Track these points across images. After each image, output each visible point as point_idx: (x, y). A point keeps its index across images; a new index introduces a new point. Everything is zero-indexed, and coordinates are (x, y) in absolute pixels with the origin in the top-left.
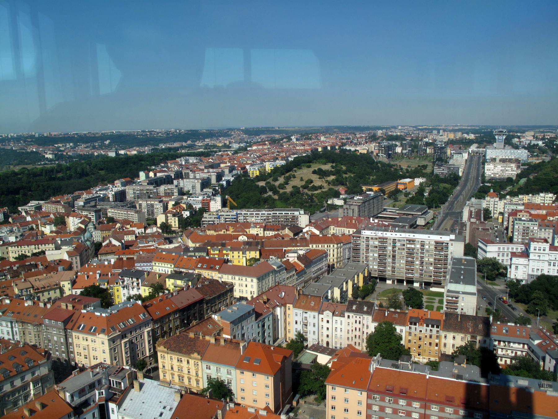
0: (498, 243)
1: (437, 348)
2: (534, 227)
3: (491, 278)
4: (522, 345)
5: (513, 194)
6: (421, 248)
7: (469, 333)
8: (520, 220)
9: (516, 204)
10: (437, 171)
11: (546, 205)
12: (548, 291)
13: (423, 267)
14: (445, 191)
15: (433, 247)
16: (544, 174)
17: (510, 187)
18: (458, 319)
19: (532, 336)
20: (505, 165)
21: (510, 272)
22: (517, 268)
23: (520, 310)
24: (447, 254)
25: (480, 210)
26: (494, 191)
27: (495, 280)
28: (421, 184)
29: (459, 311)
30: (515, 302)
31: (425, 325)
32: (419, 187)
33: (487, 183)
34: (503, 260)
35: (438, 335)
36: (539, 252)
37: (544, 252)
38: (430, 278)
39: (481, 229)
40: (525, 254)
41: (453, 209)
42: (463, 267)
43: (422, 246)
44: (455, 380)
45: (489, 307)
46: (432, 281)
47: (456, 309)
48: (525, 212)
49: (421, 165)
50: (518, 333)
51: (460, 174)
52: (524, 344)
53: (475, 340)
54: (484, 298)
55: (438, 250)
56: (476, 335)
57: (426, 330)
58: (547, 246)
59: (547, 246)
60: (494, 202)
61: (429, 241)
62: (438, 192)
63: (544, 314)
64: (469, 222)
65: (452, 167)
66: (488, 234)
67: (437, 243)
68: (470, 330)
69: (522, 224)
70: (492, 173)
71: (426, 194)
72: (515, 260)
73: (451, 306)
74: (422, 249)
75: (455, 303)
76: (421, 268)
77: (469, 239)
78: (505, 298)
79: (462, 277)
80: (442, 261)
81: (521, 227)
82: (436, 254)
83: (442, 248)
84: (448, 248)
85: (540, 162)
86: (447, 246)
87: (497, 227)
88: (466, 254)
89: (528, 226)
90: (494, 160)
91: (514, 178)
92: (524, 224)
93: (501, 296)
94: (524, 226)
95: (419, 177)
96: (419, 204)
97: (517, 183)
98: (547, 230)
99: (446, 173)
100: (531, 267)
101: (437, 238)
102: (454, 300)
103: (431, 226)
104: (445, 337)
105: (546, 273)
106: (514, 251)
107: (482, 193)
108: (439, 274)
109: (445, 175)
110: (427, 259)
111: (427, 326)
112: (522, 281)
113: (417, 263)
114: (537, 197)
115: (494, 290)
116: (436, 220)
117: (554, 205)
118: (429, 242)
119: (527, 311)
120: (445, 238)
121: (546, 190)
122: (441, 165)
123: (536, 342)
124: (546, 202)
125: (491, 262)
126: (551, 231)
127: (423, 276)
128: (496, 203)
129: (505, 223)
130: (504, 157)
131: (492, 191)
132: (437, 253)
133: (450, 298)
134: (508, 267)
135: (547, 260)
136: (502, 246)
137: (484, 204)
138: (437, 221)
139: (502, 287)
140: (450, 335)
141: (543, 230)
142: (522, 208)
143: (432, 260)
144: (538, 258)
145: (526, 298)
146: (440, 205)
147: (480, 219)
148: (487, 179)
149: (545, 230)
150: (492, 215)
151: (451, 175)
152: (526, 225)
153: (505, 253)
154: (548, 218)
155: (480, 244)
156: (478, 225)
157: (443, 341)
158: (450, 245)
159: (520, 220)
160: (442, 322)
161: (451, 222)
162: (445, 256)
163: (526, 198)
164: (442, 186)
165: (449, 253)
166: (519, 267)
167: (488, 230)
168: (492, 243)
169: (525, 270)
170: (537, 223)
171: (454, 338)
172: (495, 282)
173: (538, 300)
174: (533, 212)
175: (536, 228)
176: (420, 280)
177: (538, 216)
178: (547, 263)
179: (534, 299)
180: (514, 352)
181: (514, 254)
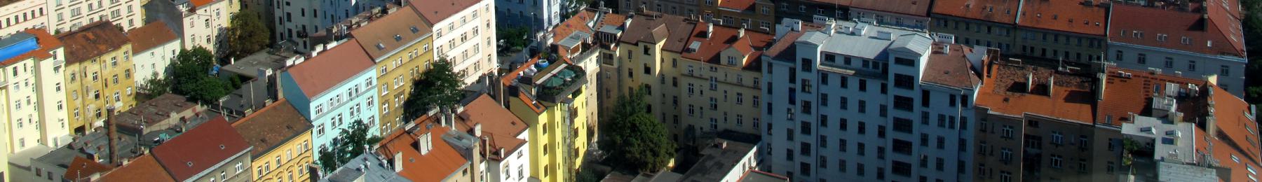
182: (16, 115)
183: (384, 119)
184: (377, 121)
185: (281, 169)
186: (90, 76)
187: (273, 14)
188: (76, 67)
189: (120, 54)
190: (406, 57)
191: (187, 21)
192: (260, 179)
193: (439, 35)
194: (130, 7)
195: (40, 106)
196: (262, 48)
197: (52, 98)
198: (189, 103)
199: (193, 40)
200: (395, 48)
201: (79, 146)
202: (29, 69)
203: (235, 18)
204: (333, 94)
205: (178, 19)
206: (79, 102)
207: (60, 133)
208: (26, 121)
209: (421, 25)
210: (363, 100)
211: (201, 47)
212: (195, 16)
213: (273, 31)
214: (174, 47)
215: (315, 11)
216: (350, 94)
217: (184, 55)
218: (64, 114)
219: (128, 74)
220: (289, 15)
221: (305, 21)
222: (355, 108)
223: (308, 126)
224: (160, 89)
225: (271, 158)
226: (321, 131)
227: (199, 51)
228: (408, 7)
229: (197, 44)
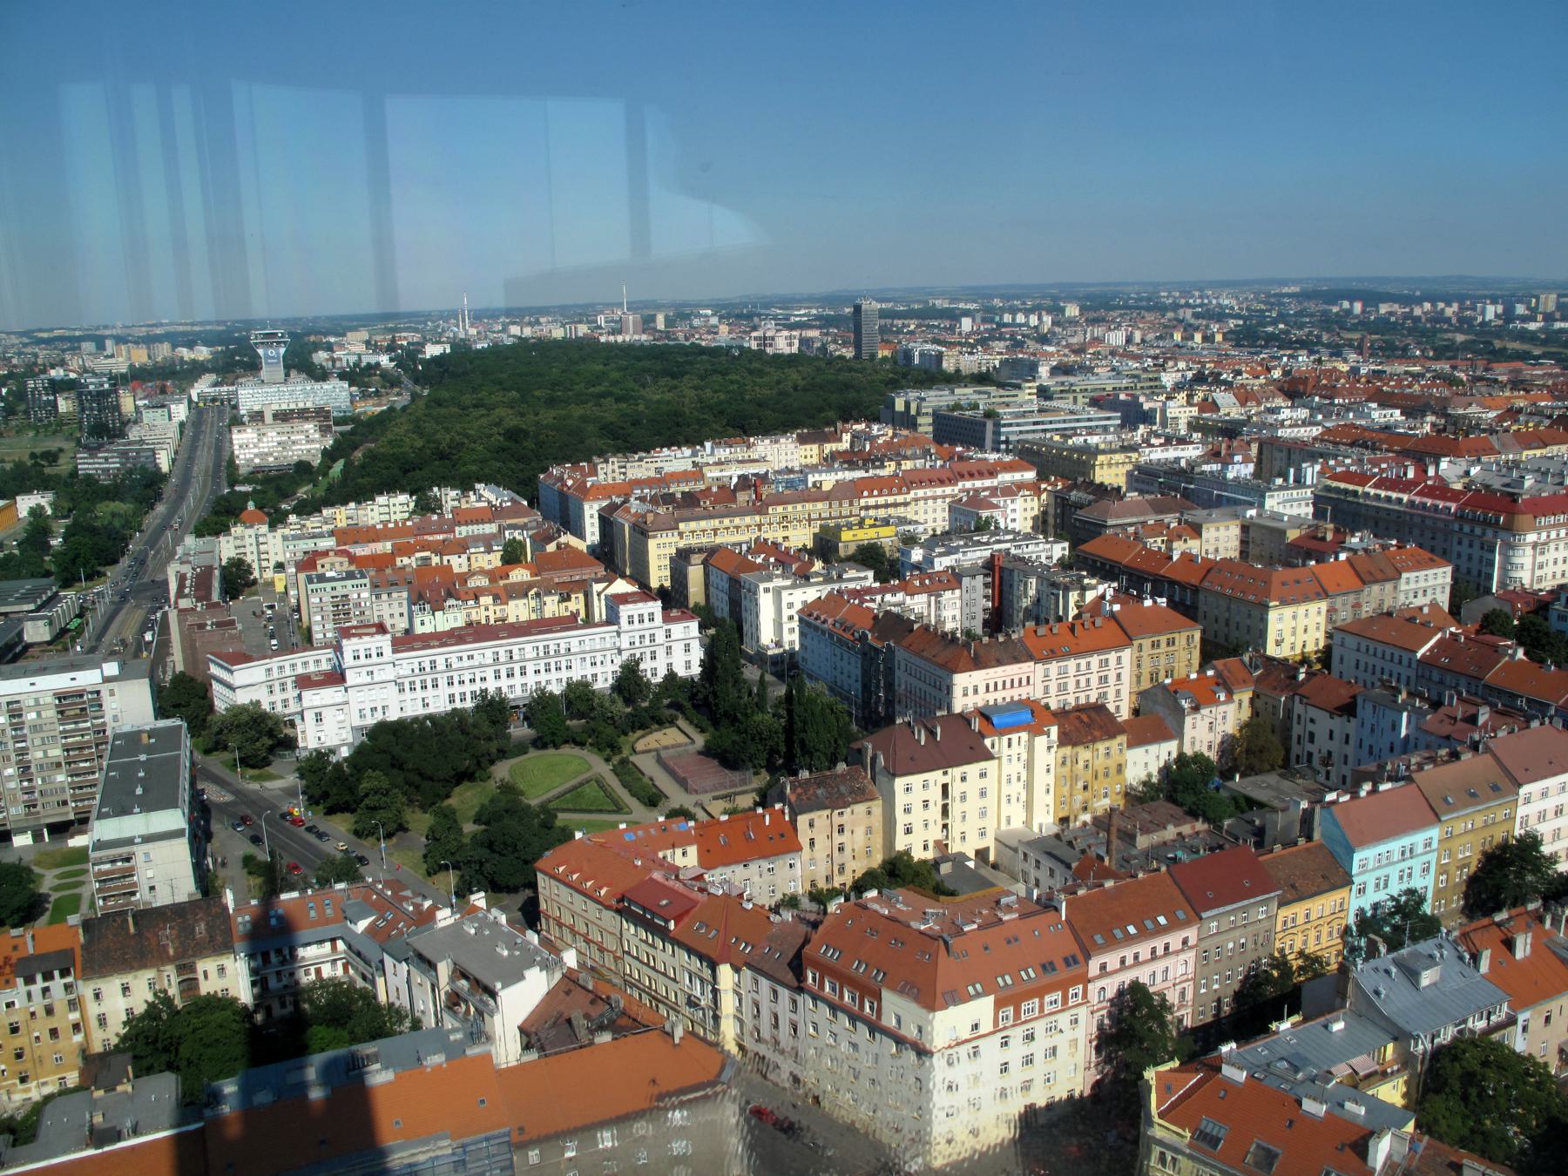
0: (276, 654)
1: (79, 1038)
2: (360, 593)
3: (254, 762)
4: (328, 945)
5: (307, 508)
6: (11, 725)
7: (170, 960)
8: (322, 578)
9: (314, 536)
10: (88, 465)
11: (391, 525)
12: (398, 764)
13: (30, 780)
14: (117, 523)
15: (50, 714)
16: (390, 442)
17: (305, 489)
18: (128, 929)
19: (348, 914)
20: (286, 427)
21: (303, 732)
22: (319, 718)
23: (338, 834)
24: (104, 724)
25: (210, 569)
26: (260, 507)
27: (269, 764)
28: (36, 512)
29: (142, 897)
30: (326, 814)
31: (20, 981)
32: (30, 524)
33: (243, 483)
34: (285, 701)
35: (72, 997)
36: (369, 661)
37: (380, 660)
38: (63, 809)
39: (213, 624)
40: (336, 677)
41: (144, 573)
42: (143, 757)
43: (13, 716)
44: (91, 1152)
45: (251, 849)
46: (72, 817)
47: (133, 894)
48: (338, 553)
49: (38, 451)
50: (313, 913)
51: (165, 468)
52: (333, 940)
53: (191, 976)
54: (239, 825)
55: (68, 717)
56: (191, 960)
57: (29, 995)
58: (385, 642)
59: (385, 642)
60: (257, 536)
61: (34, 696)
62: (94, 531)
63: (402, 828)
64: (176, 611)
65: (132, 450)
66: (232, 637)
67: (61, 696)
68: (171, 952)
69: (329, 589)
70: (256, 455)
71: (56, 542)
72: (312, 698)
73: (116, 888)
74: (17, 727)
75: (124, 877)
76: (25, 784)
77: (185, 660)
78: (296, 812)
79: (139, 791)
80: (91, 747)
81: (327, 599)
82: (65, 731)
83: (85, 709)
84: (101, 706)
85: (383, 412)
86: (98, 699)
87: (272, 607)
88: (160, 713)
89: (345, 592)
90: (257, 417)
91: (316, 462)
92: (334, 589)
93: (285, 809)
94: (334, 593)
95: (28, 491)
96: (33, 576)
97: (325, 475)
98: (395, 595)
99: (118, 469)
100: (354, 709)
101: (61, 682)
102: (120, 870)
103: (73, 640)
104: (97, 996)
105: (393, 716)
106: (300, 670)
107: (222, 515)
108: (89, 790)
109: (116, 476)
110: (40, 754)
111: (30, 980)
112: (332, 751)
113: (10, 771)
115: (266, 794)
116: (89, 615)
117: (409, 523)
118: (37, 700)
119: (357, 833)
120: (87, 678)
121: (390, 487)
122: (99, 448)
123: (362, 926)
124: (393, 517)
125: (245, 718)
126: (405, 595)
127: (39, 808)
128: (261, 540)
129: (292, 592)
130: (284, 407)
131: (251, 506)
132: (68, 727)
133: (108, 867)
134: (298, 721)
135: (392, 678)
136: (274, 663)
137: (226, 548)
138: (93, 622)
139: (291, 780)
140: (111, 986)
141: (384, 597)
142: (328, 543)
143: (56, 752)
144: (369, 679)
145: (348, 798)
146: (102, 569)
147: (208, 597)
148: (243, 471)
149: (389, 595)
150: (256, 574)
151: (130, 472)
152: (340, 592)
153: (277, 684)
154: (398, 560)
155: (214, 670)
156: (201, 615)
157: (93, 1009)
158: (105, 694)
159: (322, 578)
160: (78, 952)
161: (139, 615)
162: (99, 732)
163: (342, 515)
164: (105, 509)
165: (108, 718)
166: (326, 713)
167: (232, 623)
168: (243, 658)
169: (342, 717)
170: (366, 581)
171: (126, 989)
172: (270, 769)
173: (377, 797)
174: (361, 551)
175: (365, 595)
176: (32, 823)
178: (394, 689)
179: (367, 795)
180: (312, 969)
181: (304, 682)
182: (1006, 790)
183: (1438, 893)
184: (1430, 895)
185: (1308, 926)
186: (1081, 764)
187: (1289, 729)
188: (1067, 750)
189: (1114, 744)
190: (1479, 821)
191: (1188, 720)
192: (1284, 931)
193: (1527, 801)
194: (1118, 692)
195: (1029, 786)
196: (1273, 768)
197: (1043, 780)
198: (1189, 818)
199: (1193, 743)
200: (1466, 806)
201: (1068, 839)
202: (1023, 743)
203: (1245, 727)
204: (1382, 848)
205: (1180, 714)
206: (1066, 790)
207: (1045, 821)
208: (1013, 799)
209: (1504, 783)
210: (1416, 864)
211: (1202, 754)
212: (1198, 716)
213: (1288, 750)
214: (1164, 752)
215: (1347, 736)
216: (1403, 853)
217: (1181, 758)
218: (1050, 799)
219: (1120, 769)
220: (1312, 735)
221: (1334, 746)
222: (1407, 871)
223: (1347, 881)
224: (1153, 793)
225: (1299, 910)
226: (1362, 891)
227: (1198, 758)
228: (1488, 756)
229: (1197, 749)
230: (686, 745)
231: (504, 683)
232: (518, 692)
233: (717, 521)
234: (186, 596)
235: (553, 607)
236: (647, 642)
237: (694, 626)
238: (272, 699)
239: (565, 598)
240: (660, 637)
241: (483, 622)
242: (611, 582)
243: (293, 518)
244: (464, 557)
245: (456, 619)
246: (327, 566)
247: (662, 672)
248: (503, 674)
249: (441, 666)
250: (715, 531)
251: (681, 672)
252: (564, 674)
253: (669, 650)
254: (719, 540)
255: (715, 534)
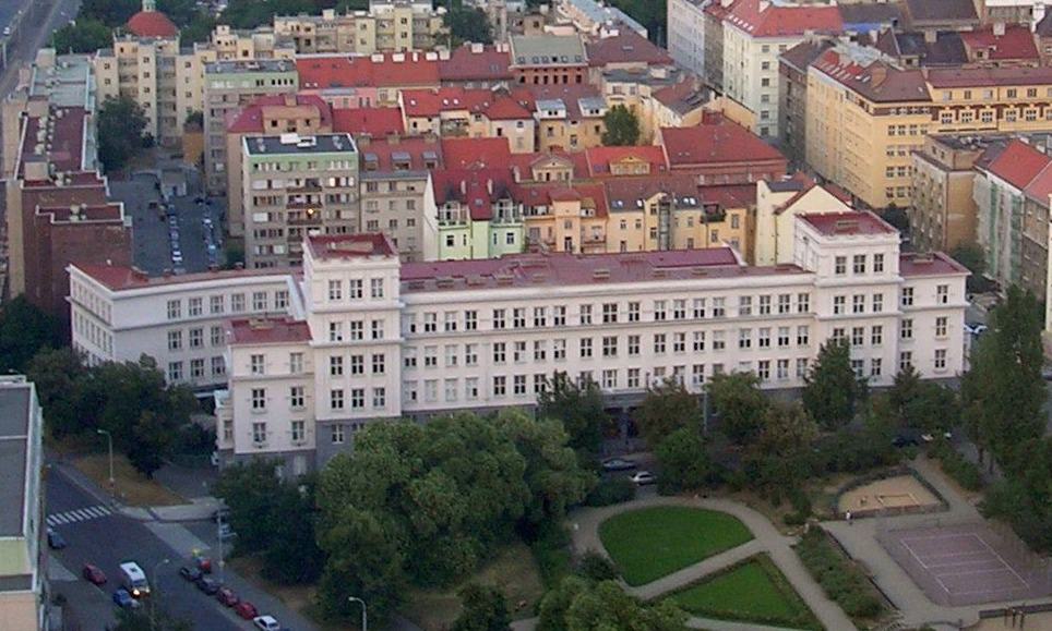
8: (274, 145)
11: (399, 58)
21: (228, 423)
34: (198, 362)
39: (81, 212)
58: (387, 269)
59: (387, 269)
98: (401, 186)
112: (284, 459)
114: (359, 22)
141: (384, 188)
150: (151, 129)
159: (274, 145)
177: (362, 117)
230: (932, 510)
231: (597, 365)
232: (622, 383)
233: (1004, 91)
234: (38, 158)
235: (689, 226)
236: (869, 310)
237: (957, 286)
238: (175, 357)
239: (714, 216)
240: (891, 304)
241: (561, 247)
242: (802, 191)
243: (223, 34)
244: (529, 125)
245: (510, 240)
246: (283, 124)
247: (890, 370)
248: (598, 347)
249: (485, 324)
250: (999, 107)
251: (925, 368)
252: (709, 358)
253: (906, 331)
254: (1005, 127)
255: (999, 116)
